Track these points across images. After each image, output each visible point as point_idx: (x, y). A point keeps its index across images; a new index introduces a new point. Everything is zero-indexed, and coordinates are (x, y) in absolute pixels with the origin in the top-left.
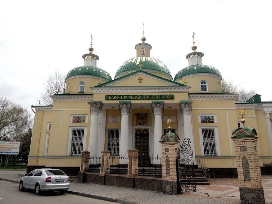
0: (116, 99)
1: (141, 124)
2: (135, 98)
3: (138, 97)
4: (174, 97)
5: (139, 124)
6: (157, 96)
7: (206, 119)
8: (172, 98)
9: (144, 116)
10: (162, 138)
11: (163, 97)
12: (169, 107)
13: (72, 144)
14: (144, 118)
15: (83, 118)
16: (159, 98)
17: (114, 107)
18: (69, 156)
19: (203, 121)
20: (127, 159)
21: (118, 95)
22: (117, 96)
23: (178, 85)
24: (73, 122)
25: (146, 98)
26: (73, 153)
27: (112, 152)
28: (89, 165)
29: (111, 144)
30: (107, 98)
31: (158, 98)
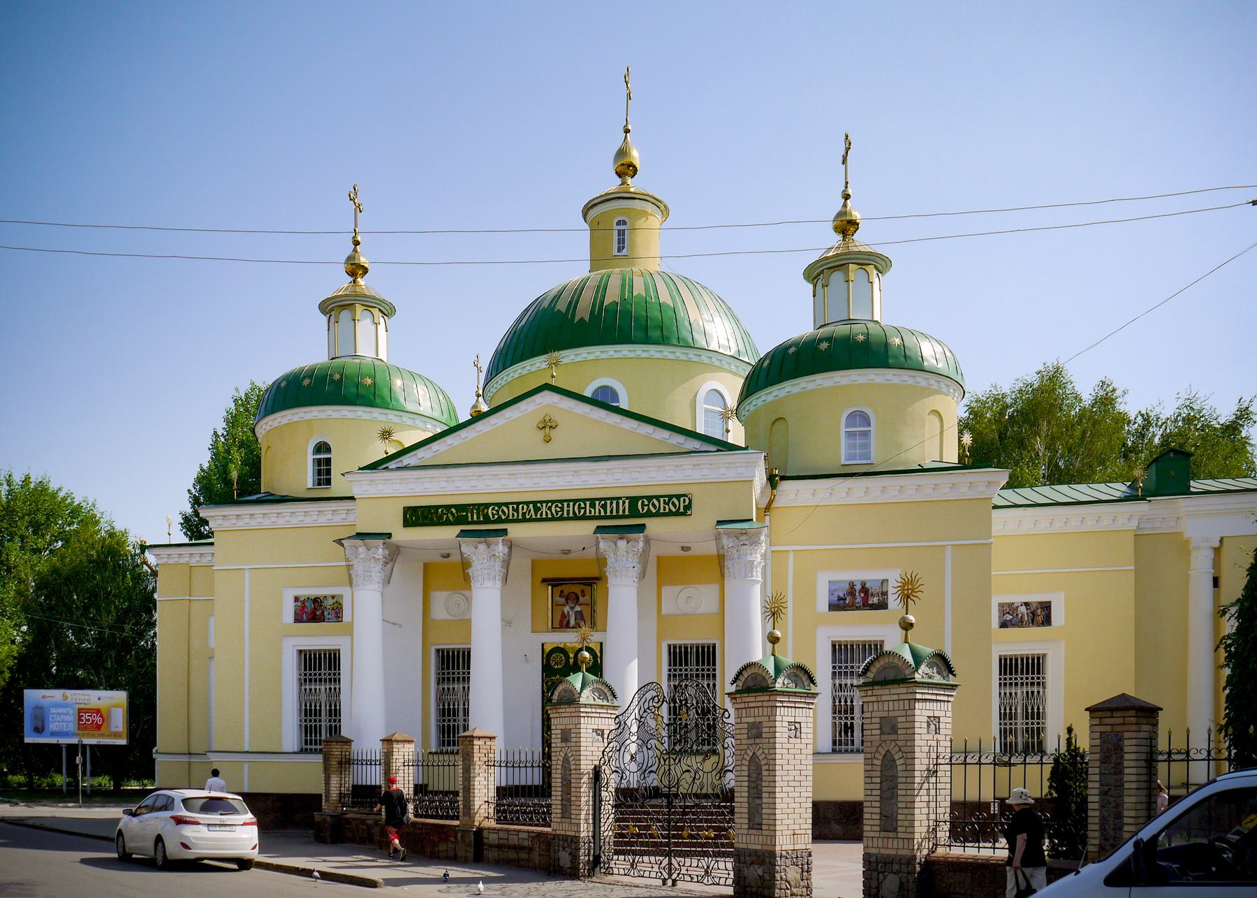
2: (524, 514)
3: (537, 510)
5: (561, 622)
6: (618, 504)
7: (852, 591)
8: (682, 510)
9: (583, 587)
11: (643, 505)
12: (683, 548)
13: (301, 706)
15: (331, 601)
16: (627, 513)
17: (448, 556)
19: (839, 605)
20: (500, 766)
21: (455, 506)
23: (713, 448)
24: (298, 619)
25: (571, 515)
26: (306, 744)
27: (454, 741)
28: (353, 786)
30: (417, 516)
31: (621, 513)
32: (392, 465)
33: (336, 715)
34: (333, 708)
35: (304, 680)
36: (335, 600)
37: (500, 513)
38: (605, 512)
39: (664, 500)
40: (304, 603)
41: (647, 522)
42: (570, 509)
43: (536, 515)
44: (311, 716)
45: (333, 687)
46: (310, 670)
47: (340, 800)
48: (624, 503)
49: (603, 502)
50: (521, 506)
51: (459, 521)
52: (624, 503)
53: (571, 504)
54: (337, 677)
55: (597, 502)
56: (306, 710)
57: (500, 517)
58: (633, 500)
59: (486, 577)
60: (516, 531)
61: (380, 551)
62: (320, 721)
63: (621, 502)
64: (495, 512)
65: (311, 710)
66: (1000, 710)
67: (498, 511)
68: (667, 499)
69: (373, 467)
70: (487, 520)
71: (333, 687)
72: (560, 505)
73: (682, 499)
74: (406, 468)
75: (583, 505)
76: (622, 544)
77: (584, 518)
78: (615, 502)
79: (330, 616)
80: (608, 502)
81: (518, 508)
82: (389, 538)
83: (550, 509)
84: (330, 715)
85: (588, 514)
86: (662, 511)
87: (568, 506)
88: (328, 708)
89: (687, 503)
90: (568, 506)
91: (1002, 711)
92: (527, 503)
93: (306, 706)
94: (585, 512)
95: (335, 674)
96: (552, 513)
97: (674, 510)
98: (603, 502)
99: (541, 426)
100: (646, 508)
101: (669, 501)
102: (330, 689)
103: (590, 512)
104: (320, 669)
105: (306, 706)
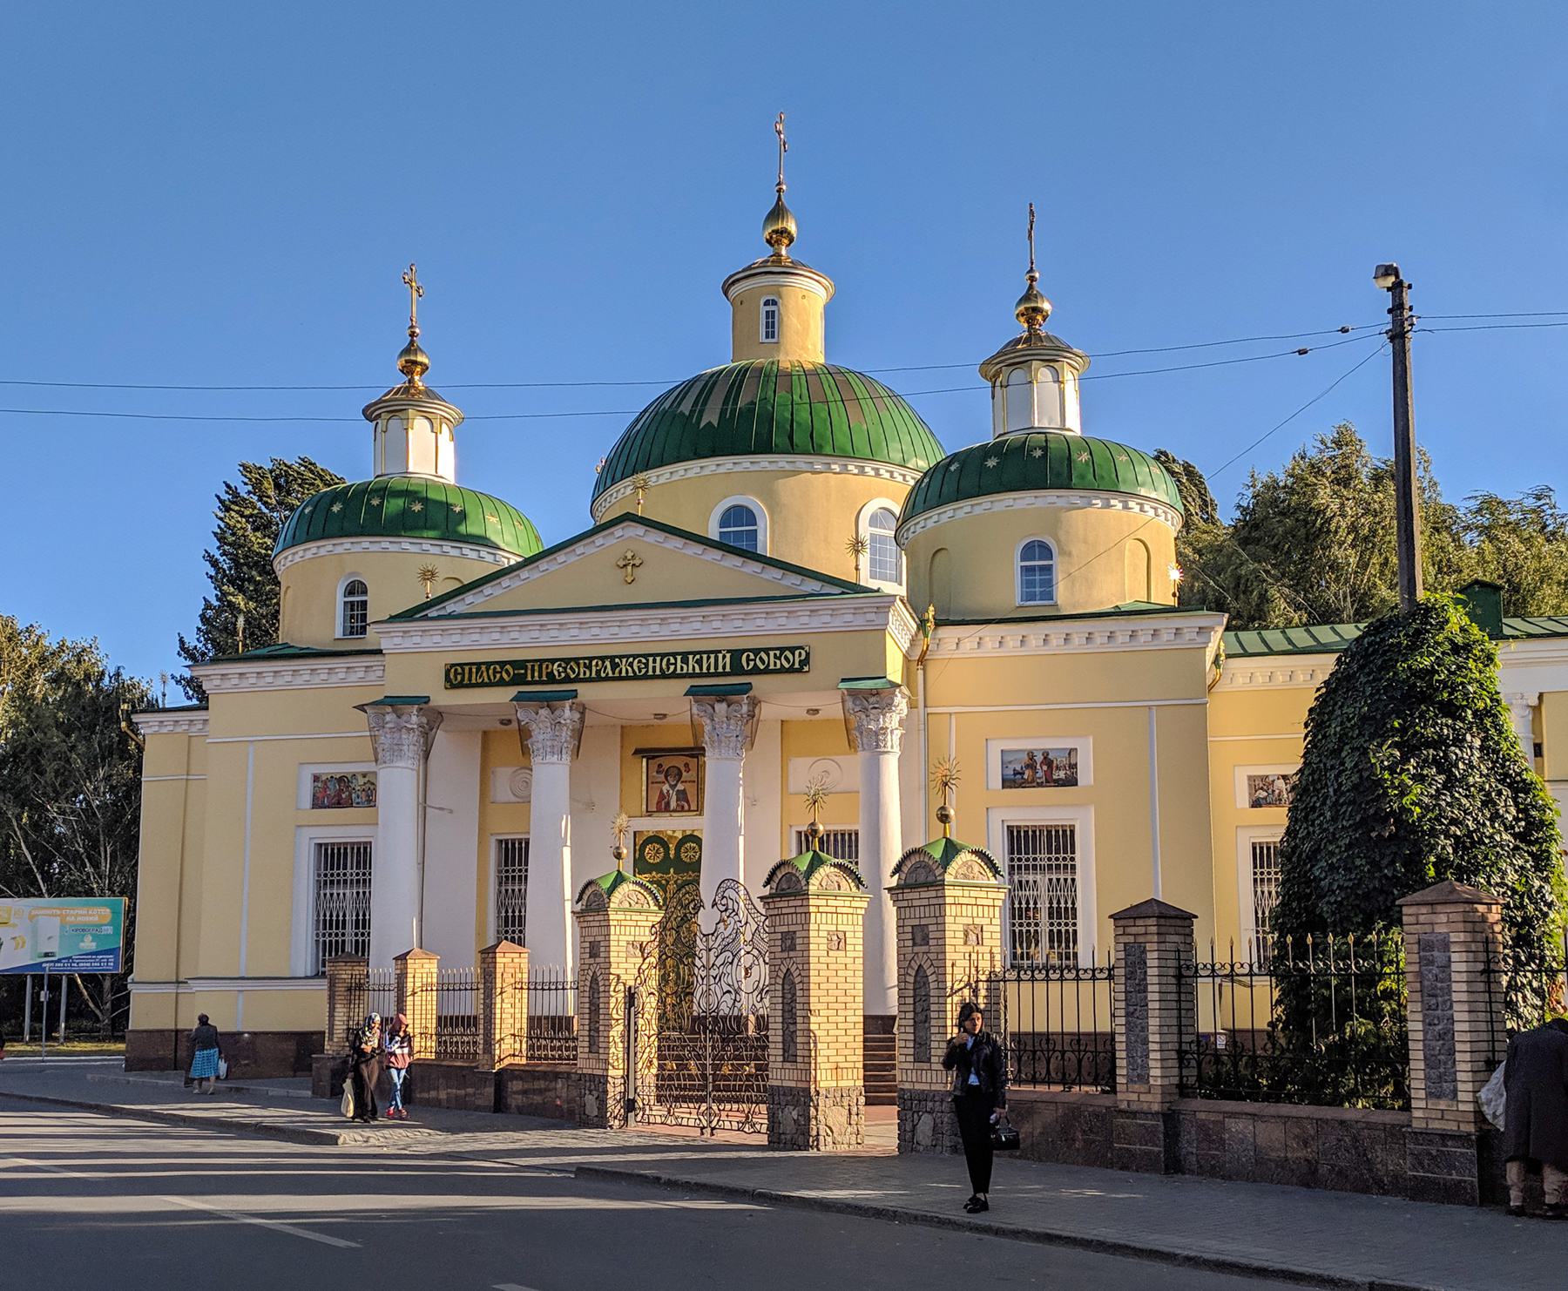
0: (501, 683)
1: (668, 804)
2: (598, 672)
3: (614, 666)
4: (805, 662)
8: (797, 666)
10: (768, 882)
13: (318, 915)
14: (684, 774)
15: (361, 781)
16: (728, 669)
18: (307, 978)
22: (502, 664)
23: (837, 590)
24: (317, 804)
25: (658, 672)
29: (514, 916)
31: (720, 670)
32: (433, 613)
33: (364, 928)
34: (361, 917)
35: (325, 882)
36: (366, 780)
37: (568, 671)
38: (701, 669)
39: (775, 654)
40: (326, 784)
41: (754, 680)
42: (657, 666)
43: (614, 673)
44: (331, 928)
45: (361, 891)
46: (332, 869)
47: (347, 1038)
48: (724, 657)
49: (698, 657)
50: (594, 663)
51: (518, 680)
52: (724, 657)
53: (658, 659)
54: (367, 877)
55: (691, 657)
56: (325, 920)
57: (567, 676)
58: (736, 654)
59: (549, 750)
60: (586, 692)
61: (414, 718)
62: (343, 935)
63: (720, 656)
64: (561, 669)
65: (331, 921)
66: (1256, 913)
67: (565, 668)
68: (778, 653)
69: (408, 616)
70: (552, 679)
71: (361, 891)
72: (644, 661)
73: (797, 652)
74: (450, 617)
75: (672, 661)
76: (721, 708)
77: (674, 676)
78: (712, 656)
79: (359, 800)
80: (705, 656)
81: (590, 663)
82: (426, 703)
83: (631, 665)
84: (357, 928)
85: (679, 671)
86: (772, 667)
87: (654, 661)
88: (354, 918)
89: (803, 658)
90: (654, 661)
91: (1260, 915)
92: (603, 659)
93: (325, 915)
94: (676, 668)
95: (364, 874)
96: (634, 671)
97: (787, 666)
98: (698, 657)
99: (621, 563)
100: (752, 663)
101: (781, 655)
102: (358, 893)
103: (682, 668)
104: (345, 868)
105: (325, 915)
